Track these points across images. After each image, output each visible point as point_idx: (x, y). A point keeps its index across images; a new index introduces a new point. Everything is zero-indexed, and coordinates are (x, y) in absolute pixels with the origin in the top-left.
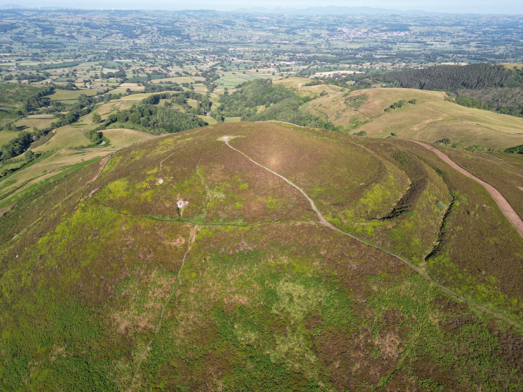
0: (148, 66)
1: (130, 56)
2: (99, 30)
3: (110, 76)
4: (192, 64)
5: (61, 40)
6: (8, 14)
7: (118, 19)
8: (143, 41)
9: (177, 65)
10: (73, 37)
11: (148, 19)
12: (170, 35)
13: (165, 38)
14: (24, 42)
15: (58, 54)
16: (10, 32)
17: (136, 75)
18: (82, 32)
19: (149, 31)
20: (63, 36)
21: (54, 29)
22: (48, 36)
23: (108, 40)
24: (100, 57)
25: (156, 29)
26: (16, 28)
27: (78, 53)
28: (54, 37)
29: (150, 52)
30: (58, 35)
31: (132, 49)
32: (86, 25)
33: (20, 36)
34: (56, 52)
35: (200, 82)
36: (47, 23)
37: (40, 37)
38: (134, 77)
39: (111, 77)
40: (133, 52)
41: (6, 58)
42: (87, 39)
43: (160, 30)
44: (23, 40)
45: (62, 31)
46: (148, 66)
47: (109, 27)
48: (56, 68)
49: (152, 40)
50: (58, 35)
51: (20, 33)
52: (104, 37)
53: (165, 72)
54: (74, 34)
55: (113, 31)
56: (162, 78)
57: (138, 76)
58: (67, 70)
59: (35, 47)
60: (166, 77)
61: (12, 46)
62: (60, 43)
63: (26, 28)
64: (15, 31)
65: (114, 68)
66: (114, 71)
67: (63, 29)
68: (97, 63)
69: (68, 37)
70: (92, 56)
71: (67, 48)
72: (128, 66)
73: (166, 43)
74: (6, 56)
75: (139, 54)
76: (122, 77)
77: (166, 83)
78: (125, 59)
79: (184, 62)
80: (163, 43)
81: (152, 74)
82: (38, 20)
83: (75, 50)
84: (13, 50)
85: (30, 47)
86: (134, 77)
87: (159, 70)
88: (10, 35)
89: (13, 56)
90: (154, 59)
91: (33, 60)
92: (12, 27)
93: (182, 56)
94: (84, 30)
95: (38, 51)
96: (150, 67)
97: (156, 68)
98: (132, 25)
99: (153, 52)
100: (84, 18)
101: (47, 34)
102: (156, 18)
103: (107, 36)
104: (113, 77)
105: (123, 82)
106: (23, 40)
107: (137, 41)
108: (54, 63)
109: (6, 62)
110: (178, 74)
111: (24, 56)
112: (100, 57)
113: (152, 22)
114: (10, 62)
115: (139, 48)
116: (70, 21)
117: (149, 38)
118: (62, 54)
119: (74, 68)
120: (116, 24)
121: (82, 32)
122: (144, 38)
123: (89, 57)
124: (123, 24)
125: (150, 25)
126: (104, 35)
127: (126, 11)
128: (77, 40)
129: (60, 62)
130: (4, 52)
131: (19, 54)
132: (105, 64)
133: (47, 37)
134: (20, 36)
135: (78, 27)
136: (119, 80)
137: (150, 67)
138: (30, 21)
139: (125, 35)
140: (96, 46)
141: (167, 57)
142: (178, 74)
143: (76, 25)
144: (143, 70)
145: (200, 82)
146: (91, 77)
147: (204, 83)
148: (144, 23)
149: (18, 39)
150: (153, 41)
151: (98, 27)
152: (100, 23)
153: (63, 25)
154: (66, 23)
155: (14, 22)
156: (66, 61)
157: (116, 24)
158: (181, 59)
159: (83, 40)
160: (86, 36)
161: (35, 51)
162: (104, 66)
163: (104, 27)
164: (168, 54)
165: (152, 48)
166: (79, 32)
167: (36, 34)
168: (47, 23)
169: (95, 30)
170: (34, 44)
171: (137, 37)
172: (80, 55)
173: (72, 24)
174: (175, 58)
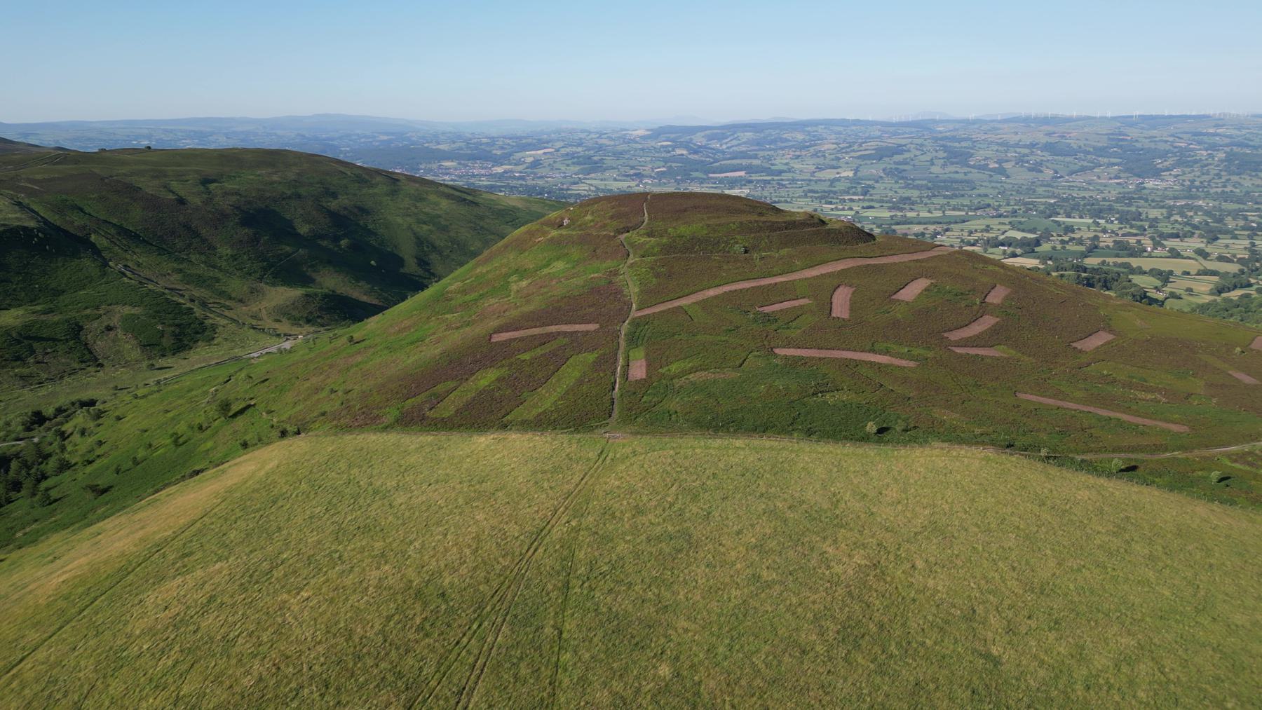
0: (1120, 233)
1: (1097, 213)
2: (1068, 159)
3: (1009, 243)
4: (1250, 237)
5: (975, 175)
6: (908, 130)
7: (1133, 133)
8: (1164, 185)
9: (1201, 236)
10: (1001, 171)
11: (1218, 135)
12: (1256, 170)
13: (1235, 178)
14: (902, 178)
15: (945, 201)
16: (887, 159)
17: (1059, 247)
18: (1028, 162)
19: (1196, 162)
20: (982, 168)
21: (972, 155)
22: (952, 168)
23: (1079, 179)
24: (1028, 210)
25: (1222, 155)
26: (901, 152)
27: (988, 201)
28: (966, 169)
29: (1163, 207)
30: (973, 167)
31: (1118, 200)
32: (1048, 147)
33: (902, 167)
34: (945, 197)
35: (1214, 273)
36: (964, 144)
37: (936, 170)
38: (1054, 248)
39: (1003, 245)
40: (1118, 206)
41: (852, 204)
42: (1031, 176)
43: (1230, 158)
44: (904, 174)
45: (986, 159)
46: (1120, 233)
47: (1101, 151)
48: (919, 223)
49: (1193, 181)
50: (973, 167)
51: (905, 163)
52: (1071, 173)
53: (1148, 244)
54: (1005, 165)
55: (1106, 160)
56: (1117, 256)
57: (1064, 248)
58: (931, 228)
59: (918, 187)
60: (1131, 255)
61: (876, 185)
62: (967, 182)
63: (919, 153)
64: (897, 158)
65: (1033, 231)
66: (1019, 235)
67: (989, 153)
68: (1007, 220)
69: (991, 170)
70: (1010, 208)
71: (975, 192)
72: (1069, 229)
73: (1228, 189)
74: (852, 200)
75: (1133, 209)
76: (1030, 248)
77: (1115, 264)
78: (1081, 217)
79: (1227, 232)
80: (1219, 190)
81: (1108, 247)
82: (954, 139)
83: (986, 196)
84: (872, 191)
85: (907, 186)
86: (1054, 248)
87: (1138, 242)
88: (883, 166)
89: (863, 200)
90: (1156, 220)
91: (890, 209)
92: (899, 150)
93: (1245, 218)
94: (1033, 158)
95: (915, 194)
96: (1124, 235)
97: (1132, 240)
98: (1162, 146)
99: (1170, 208)
100: (1049, 134)
101: (952, 163)
102: (1244, 132)
103: (1083, 169)
104: (1010, 245)
105: (1014, 255)
106: (904, 174)
107: (1150, 183)
108: (924, 214)
109: (843, 209)
110: (1175, 254)
111: (882, 201)
112: (1028, 210)
113: (1228, 141)
114: (851, 209)
115: (1141, 198)
116: (1013, 139)
117: (1190, 176)
118: (953, 202)
119: (952, 226)
120: (1121, 147)
121: (1028, 162)
122: (1176, 176)
123: (1002, 211)
124: (1139, 145)
125: (1214, 147)
126: (1076, 167)
127: (1171, 117)
128: (1008, 177)
129: (939, 214)
130: (855, 194)
131: (874, 197)
132: (1020, 223)
133: (954, 171)
134: (902, 167)
135: (1027, 151)
136: (1009, 250)
137: (1124, 235)
138: (936, 139)
139: (1127, 170)
140: (1040, 190)
141: (1196, 220)
142: (1175, 254)
143: (1025, 146)
144: (1096, 238)
145: (1214, 273)
146: (962, 241)
147: (1224, 276)
148: (1199, 143)
149: (896, 173)
150: (1197, 183)
151: (1072, 153)
152: (1081, 143)
153: (996, 148)
154: (1005, 144)
155: (903, 142)
156: (948, 213)
157: (1121, 147)
158: (1230, 223)
159: (1021, 176)
160: (1030, 170)
161: (907, 193)
162: (1013, 226)
163: (1089, 153)
164: (1207, 213)
165: (1175, 198)
166: (1020, 161)
167: (933, 164)
168: (964, 144)
169: (1060, 158)
170: (917, 182)
171: (1157, 174)
172: (989, 205)
173: (1017, 145)
174: (1220, 221)
